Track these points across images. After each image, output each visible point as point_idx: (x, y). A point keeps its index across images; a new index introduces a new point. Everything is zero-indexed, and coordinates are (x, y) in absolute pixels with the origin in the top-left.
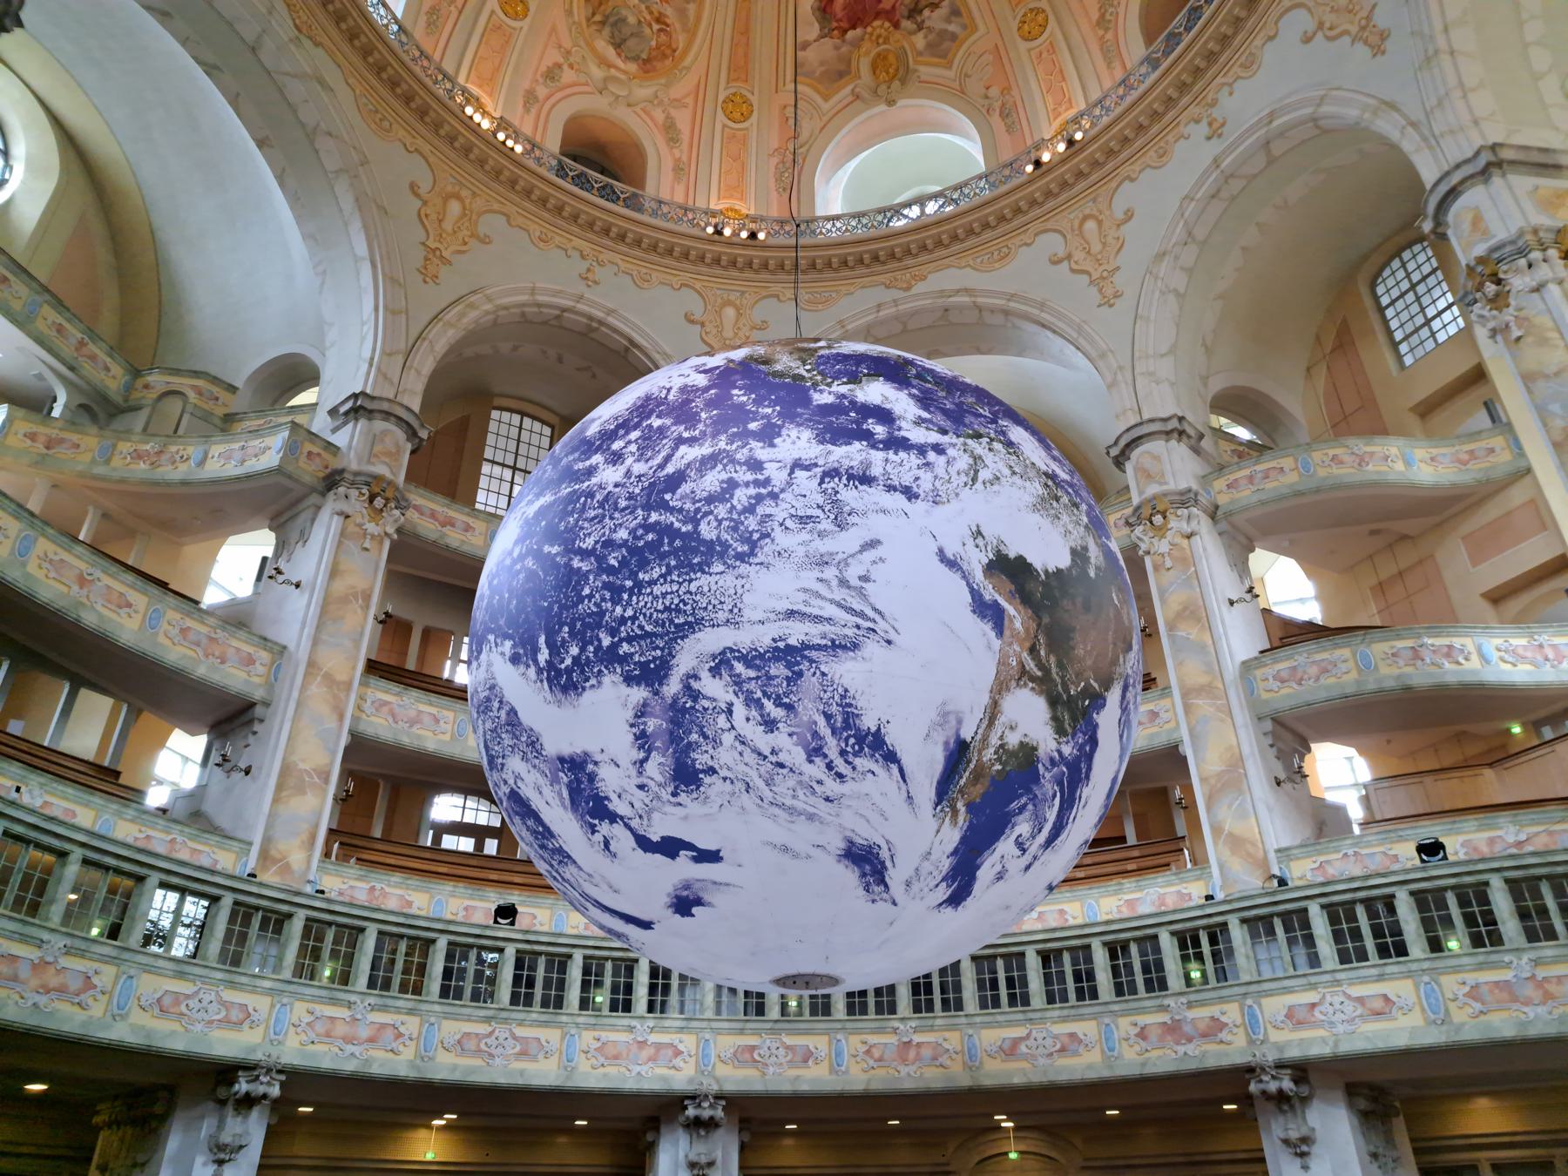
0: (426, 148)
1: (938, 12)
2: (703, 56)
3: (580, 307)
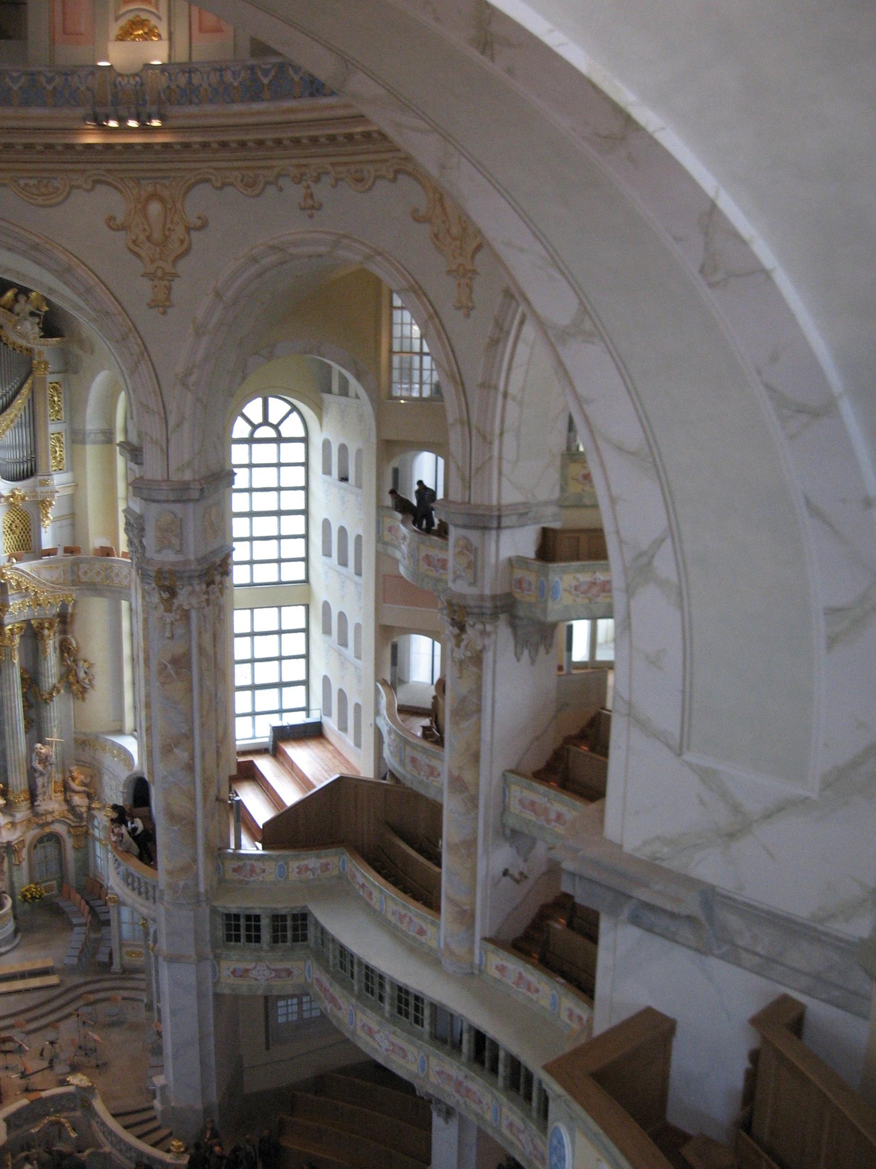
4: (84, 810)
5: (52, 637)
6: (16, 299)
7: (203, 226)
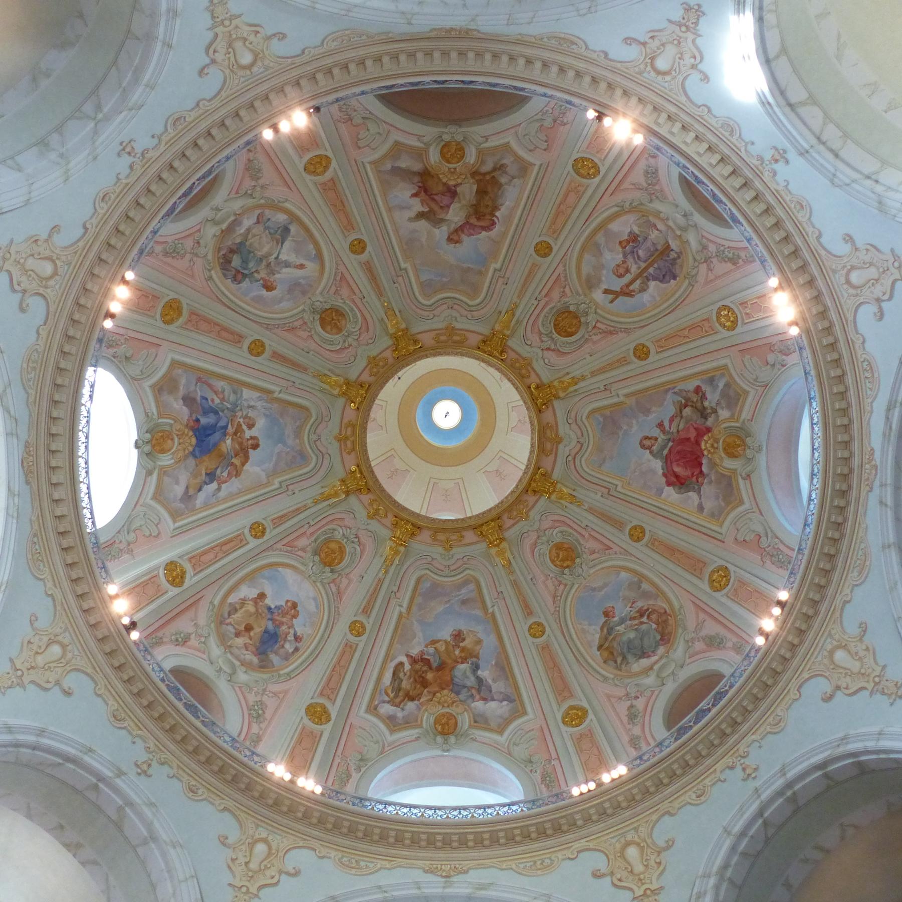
0: (583, 843)
1: (708, 395)
2: (680, 591)
3: (765, 796)
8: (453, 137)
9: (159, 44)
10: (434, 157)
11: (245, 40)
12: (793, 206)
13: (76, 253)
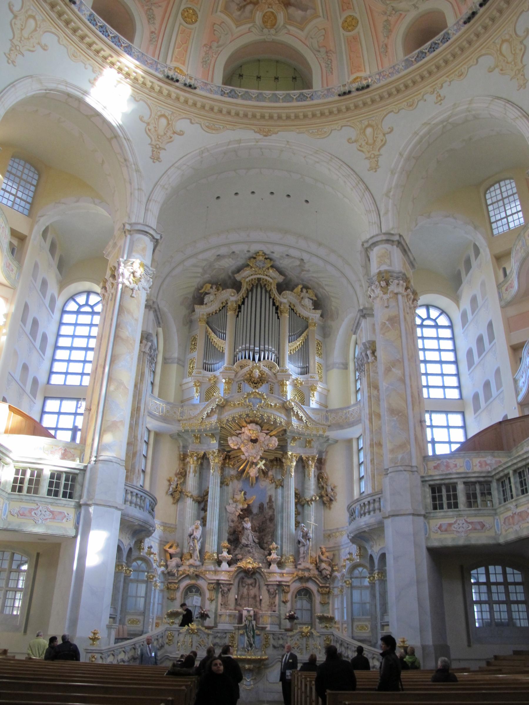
4: (328, 572)
5: (313, 467)
6: (302, 291)
7: (392, 130)
8: (269, 32)
9: (404, 156)
10: (281, 17)
11: (367, 143)
12: (79, 53)
13: (488, 48)
